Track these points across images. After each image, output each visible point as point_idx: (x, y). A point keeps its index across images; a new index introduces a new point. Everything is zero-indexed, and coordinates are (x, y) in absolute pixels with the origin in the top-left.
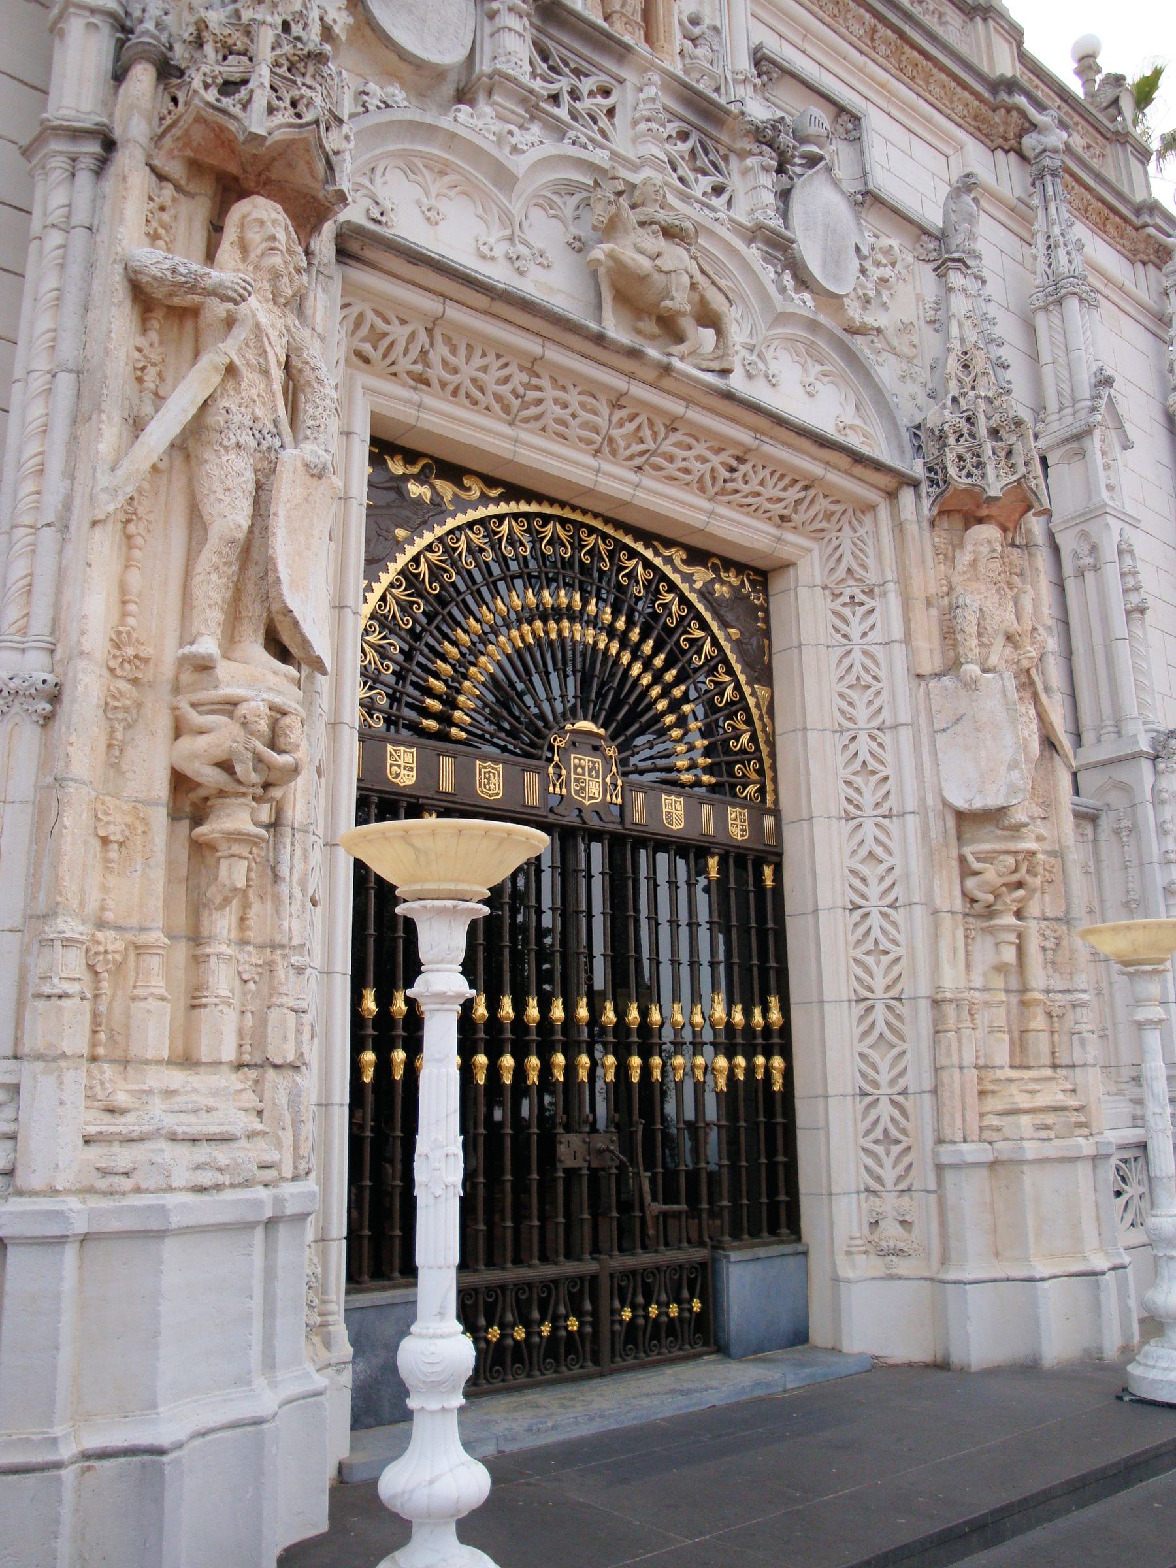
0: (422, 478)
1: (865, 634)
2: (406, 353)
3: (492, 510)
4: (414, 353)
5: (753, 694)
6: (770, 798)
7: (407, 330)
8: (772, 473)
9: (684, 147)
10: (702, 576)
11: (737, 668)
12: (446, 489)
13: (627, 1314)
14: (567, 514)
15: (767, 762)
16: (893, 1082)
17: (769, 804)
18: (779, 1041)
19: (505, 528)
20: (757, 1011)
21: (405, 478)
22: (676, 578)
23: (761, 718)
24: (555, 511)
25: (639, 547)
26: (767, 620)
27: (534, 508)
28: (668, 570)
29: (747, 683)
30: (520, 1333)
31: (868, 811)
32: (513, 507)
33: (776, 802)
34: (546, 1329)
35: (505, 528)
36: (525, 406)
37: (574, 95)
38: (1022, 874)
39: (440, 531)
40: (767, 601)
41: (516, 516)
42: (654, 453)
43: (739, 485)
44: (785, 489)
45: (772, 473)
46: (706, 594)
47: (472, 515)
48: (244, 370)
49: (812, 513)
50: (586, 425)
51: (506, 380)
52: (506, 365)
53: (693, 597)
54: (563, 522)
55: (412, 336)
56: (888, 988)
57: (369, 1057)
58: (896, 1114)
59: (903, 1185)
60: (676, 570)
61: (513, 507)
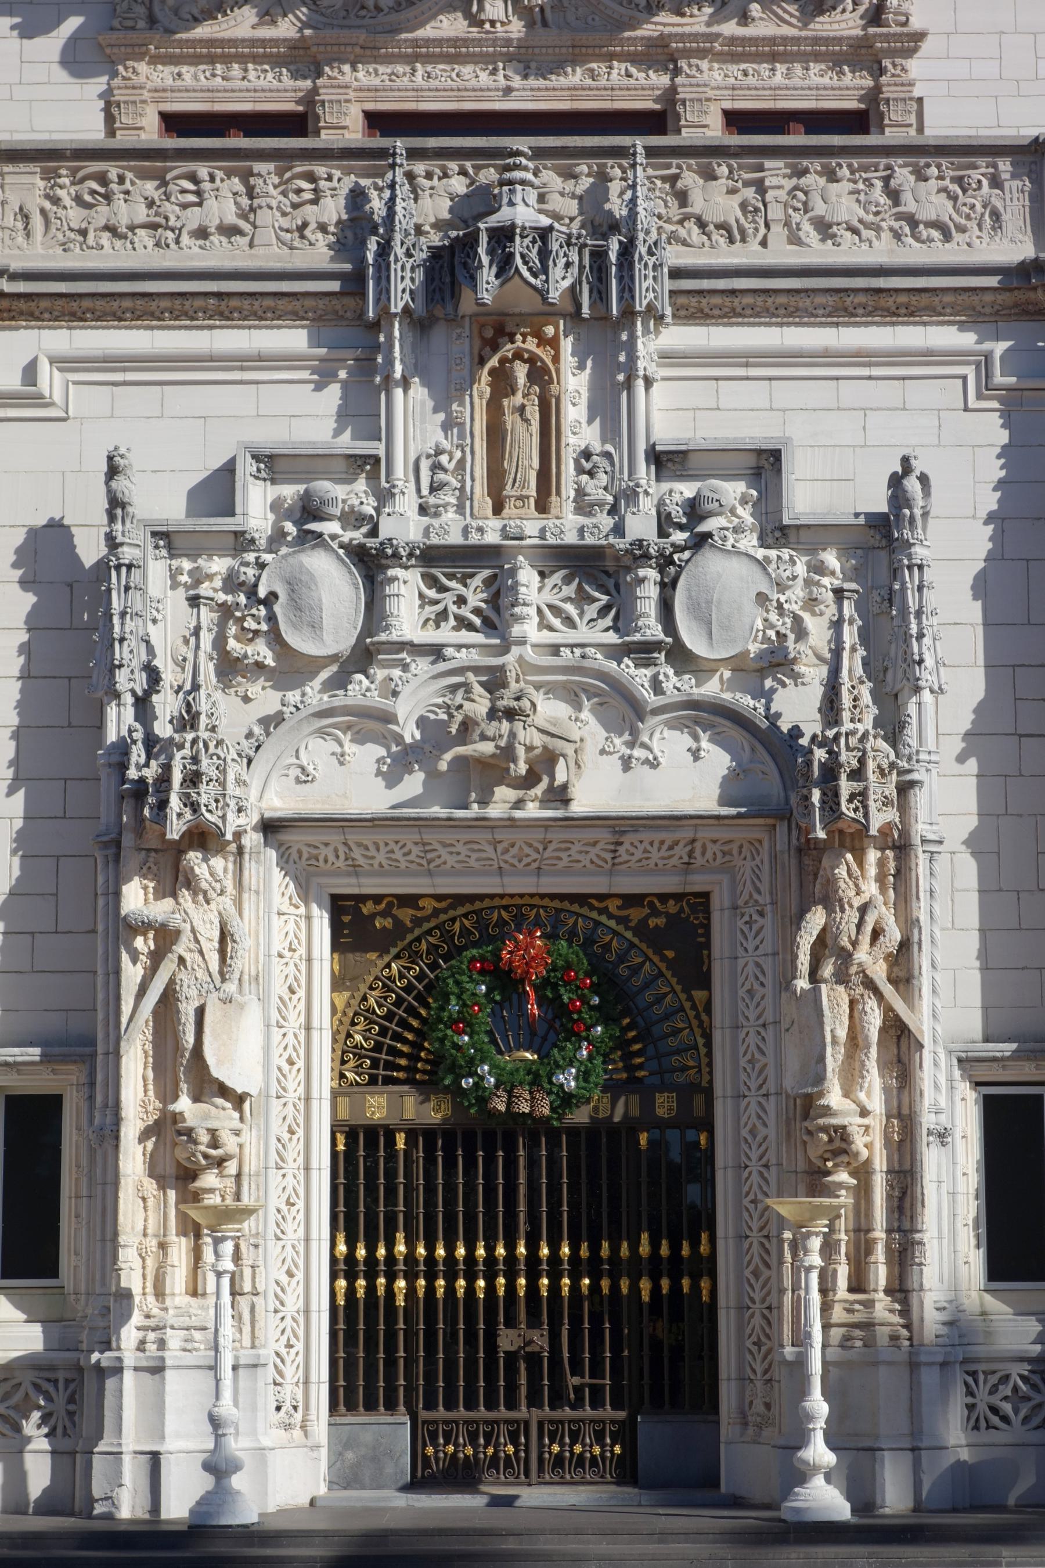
0: (384, 914)
1: (757, 948)
2: (337, 857)
3: (443, 917)
4: (342, 856)
5: (690, 998)
6: (706, 1078)
7: (331, 848)
8: (651, 844)
9: (570, 590)
10: (635, 914)
11: (674, 981)
12: (406, 915)
13: (556, 1448)
14: (505, 902)
15: (703, 1051)
16: (763, 1300)
17: (704, 1084)
18: (708, 1267)
19: (457, 926)
20: (685, 1245)
21: (373, 916)
22: (612, 923)
23: (698, 1017)
24: (497, 902)
25: (575, 908)
26: (708, 934)
27: (478, 905)
28: (603, 919)
29: (683, 991)
30: (469, 1451)
31: (753, 1093)
32: (461, 910)
33: (711, 1082)
34: (490, 1451)
35: (457, 925)
36: (429, 862)
37: (461, 601)
38: (837, 1144)
39: (401, 945)
40: (708, 919)
41: (465, 916)
42: (542, 860)
43: (625, 857)
44: (671, 848)
45: (651, 844)
46: (641, 929)
47: (426, 926)
48: (187, 956)
49: (709, 855)
50: (478, 860)
51: (409, 853)
52: (404, 845)
53: (629, 935)
54: (506, 908)
55: (336, 850)
56: (761, 1229)
57: (342, 1283)
58: (764, 1323)
59: (767, 1377)
60: (610, 916)
61: (461, 910)
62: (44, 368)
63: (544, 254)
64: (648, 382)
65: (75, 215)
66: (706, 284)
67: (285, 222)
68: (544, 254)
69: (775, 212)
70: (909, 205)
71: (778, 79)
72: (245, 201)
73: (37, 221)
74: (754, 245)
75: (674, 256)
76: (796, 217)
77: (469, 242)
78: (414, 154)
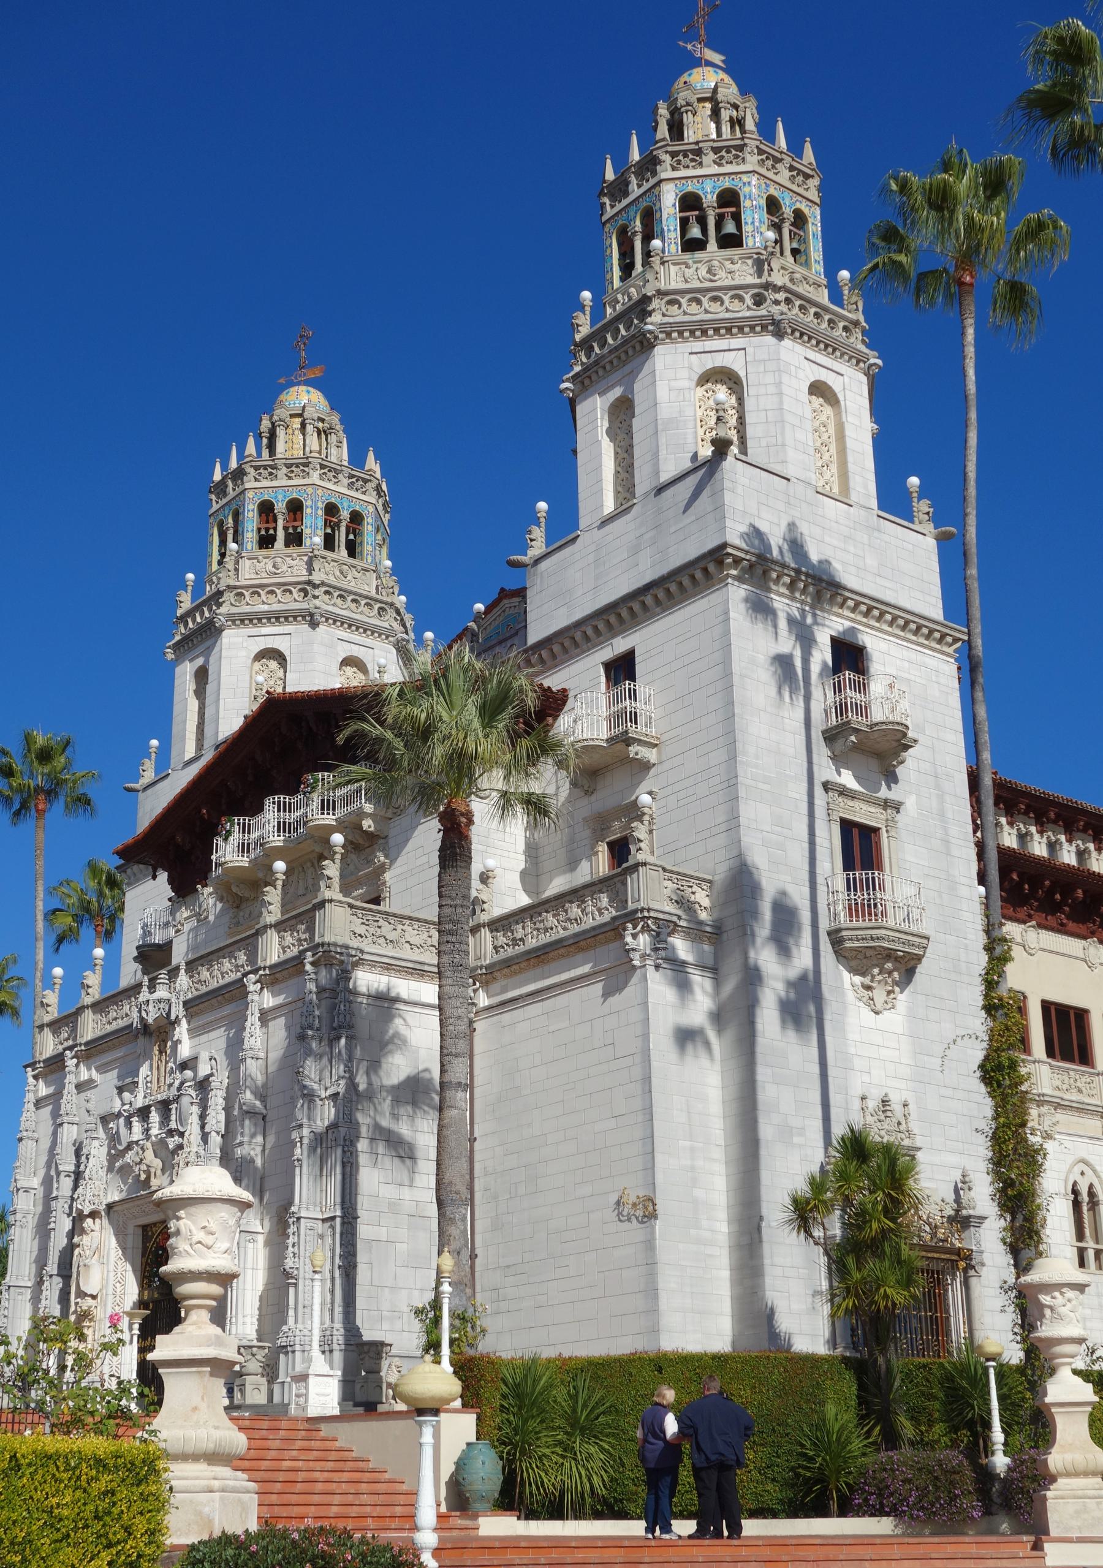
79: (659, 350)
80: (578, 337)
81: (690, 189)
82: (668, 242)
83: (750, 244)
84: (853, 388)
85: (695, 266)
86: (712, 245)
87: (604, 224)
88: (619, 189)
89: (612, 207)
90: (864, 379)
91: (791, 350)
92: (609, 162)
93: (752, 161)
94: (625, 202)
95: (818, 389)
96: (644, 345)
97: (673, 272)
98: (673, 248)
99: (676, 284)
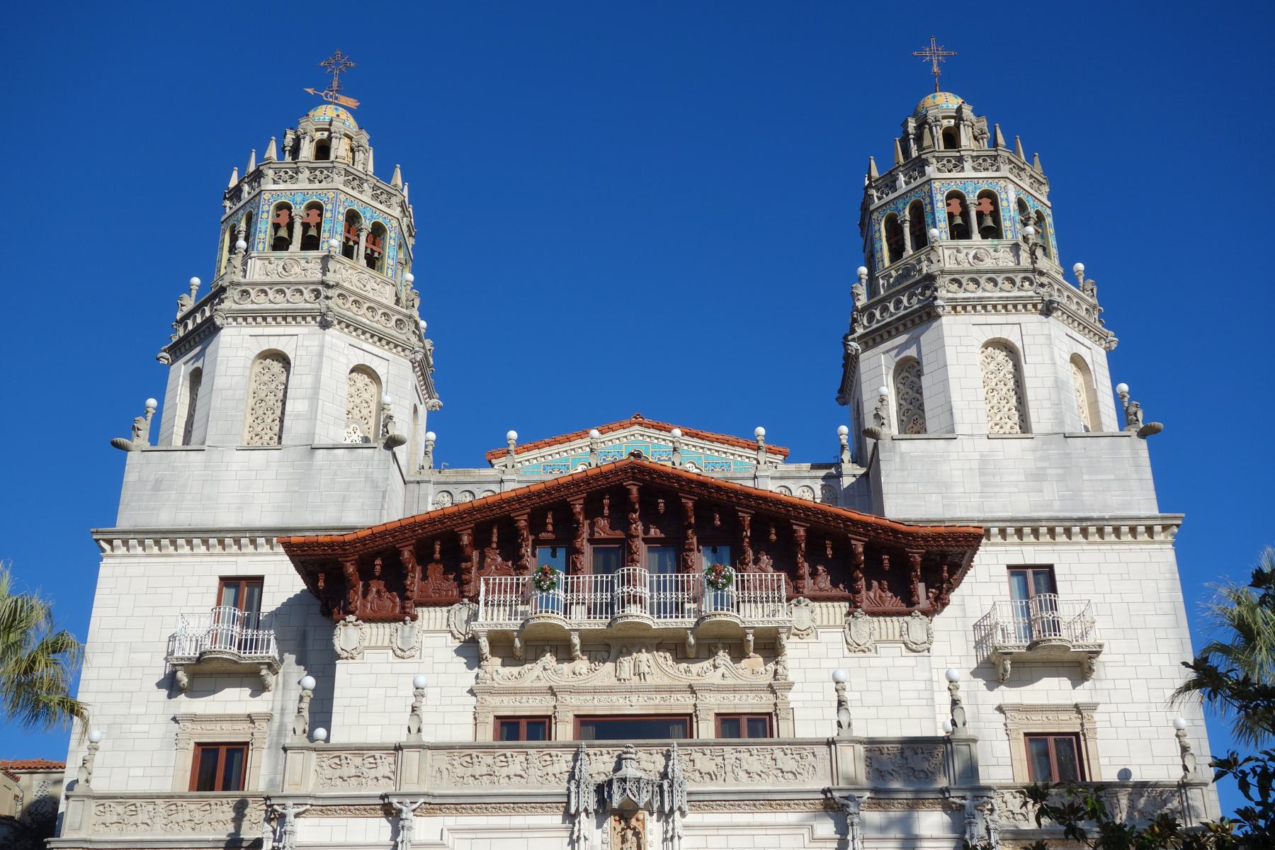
62: (445, 833)
63: (638, 789)
64: (679, 838)
65: (460, 771)
66: (701, 798)
67: (540, 773)
68: (638, 789)
69: (728, 768)
70: (780, 765)
71: (737, 701)
72: (525, 765)
73: (445, 772)
74: (721, 780)
75: (690, 787)
76: (736, 770)
77: (610, 783)
78: (589, 746)
79: (944, 319)
80: (859, 304)
81: (954, 188)
82: (938, 232)
83: (1010, 236)
84: (1097, 357)
85: (965, 251)
86: (976, 236)
87: (872, 212)
88: (889, 183)
89: (879, 199)
90: (1104, 353)
91: (1055, 326)
92: (873, 162)
93: (1005, 170)
94: (892, 196)
95: (1077, 360)
96: (927, 315)
97: (948, 254)
98: (944, 236)
99: (950, 265)
